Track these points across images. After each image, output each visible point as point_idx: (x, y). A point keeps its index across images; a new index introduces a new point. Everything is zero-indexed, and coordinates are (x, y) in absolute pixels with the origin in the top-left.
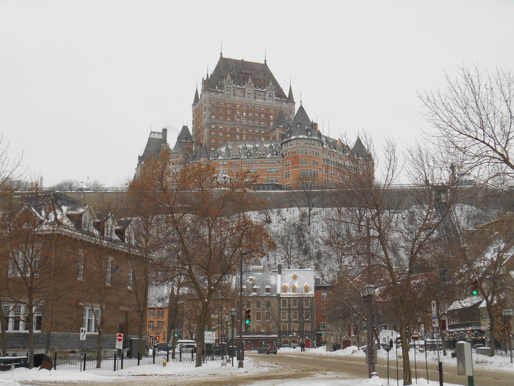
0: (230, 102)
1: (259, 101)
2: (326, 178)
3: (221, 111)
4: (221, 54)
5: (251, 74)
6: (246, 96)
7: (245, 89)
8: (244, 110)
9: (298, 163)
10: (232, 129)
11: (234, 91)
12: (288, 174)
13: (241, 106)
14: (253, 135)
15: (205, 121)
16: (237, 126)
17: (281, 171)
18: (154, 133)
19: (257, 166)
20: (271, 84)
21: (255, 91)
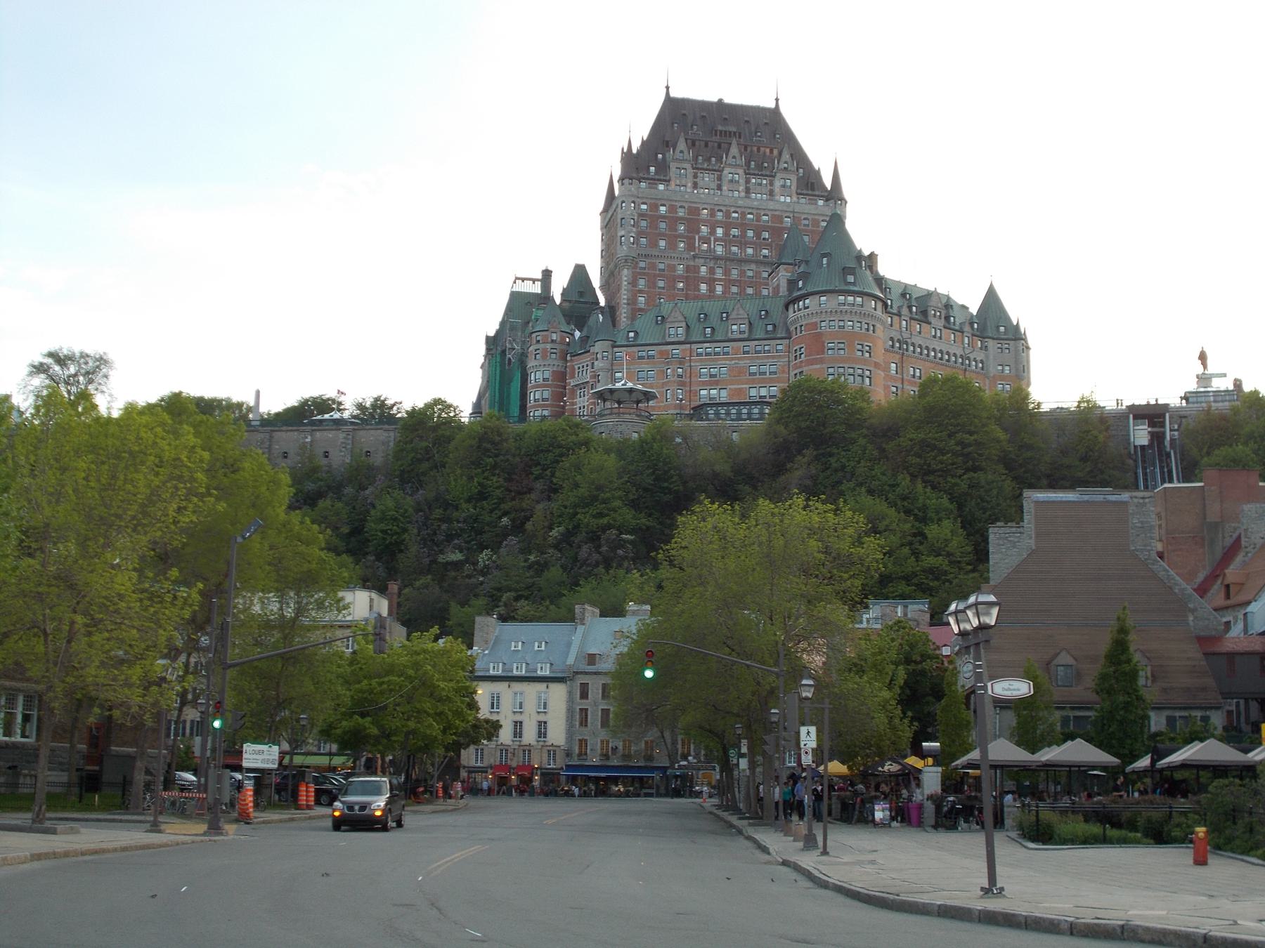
0: (684, 204)
1: (758, 197)
2: (900, 386)
3: (663, 225)
4: (667, 88)
5: (740, 134)
6: (725, 188)
8: (717, 222)
10: (688, 269)
11: (695, 176)
13: (712, 213)
14: (740, 281)
15: (622, 251)
16: (702, 261)
17: (783, 372)
18: (523, 280)
20: (786, 156)
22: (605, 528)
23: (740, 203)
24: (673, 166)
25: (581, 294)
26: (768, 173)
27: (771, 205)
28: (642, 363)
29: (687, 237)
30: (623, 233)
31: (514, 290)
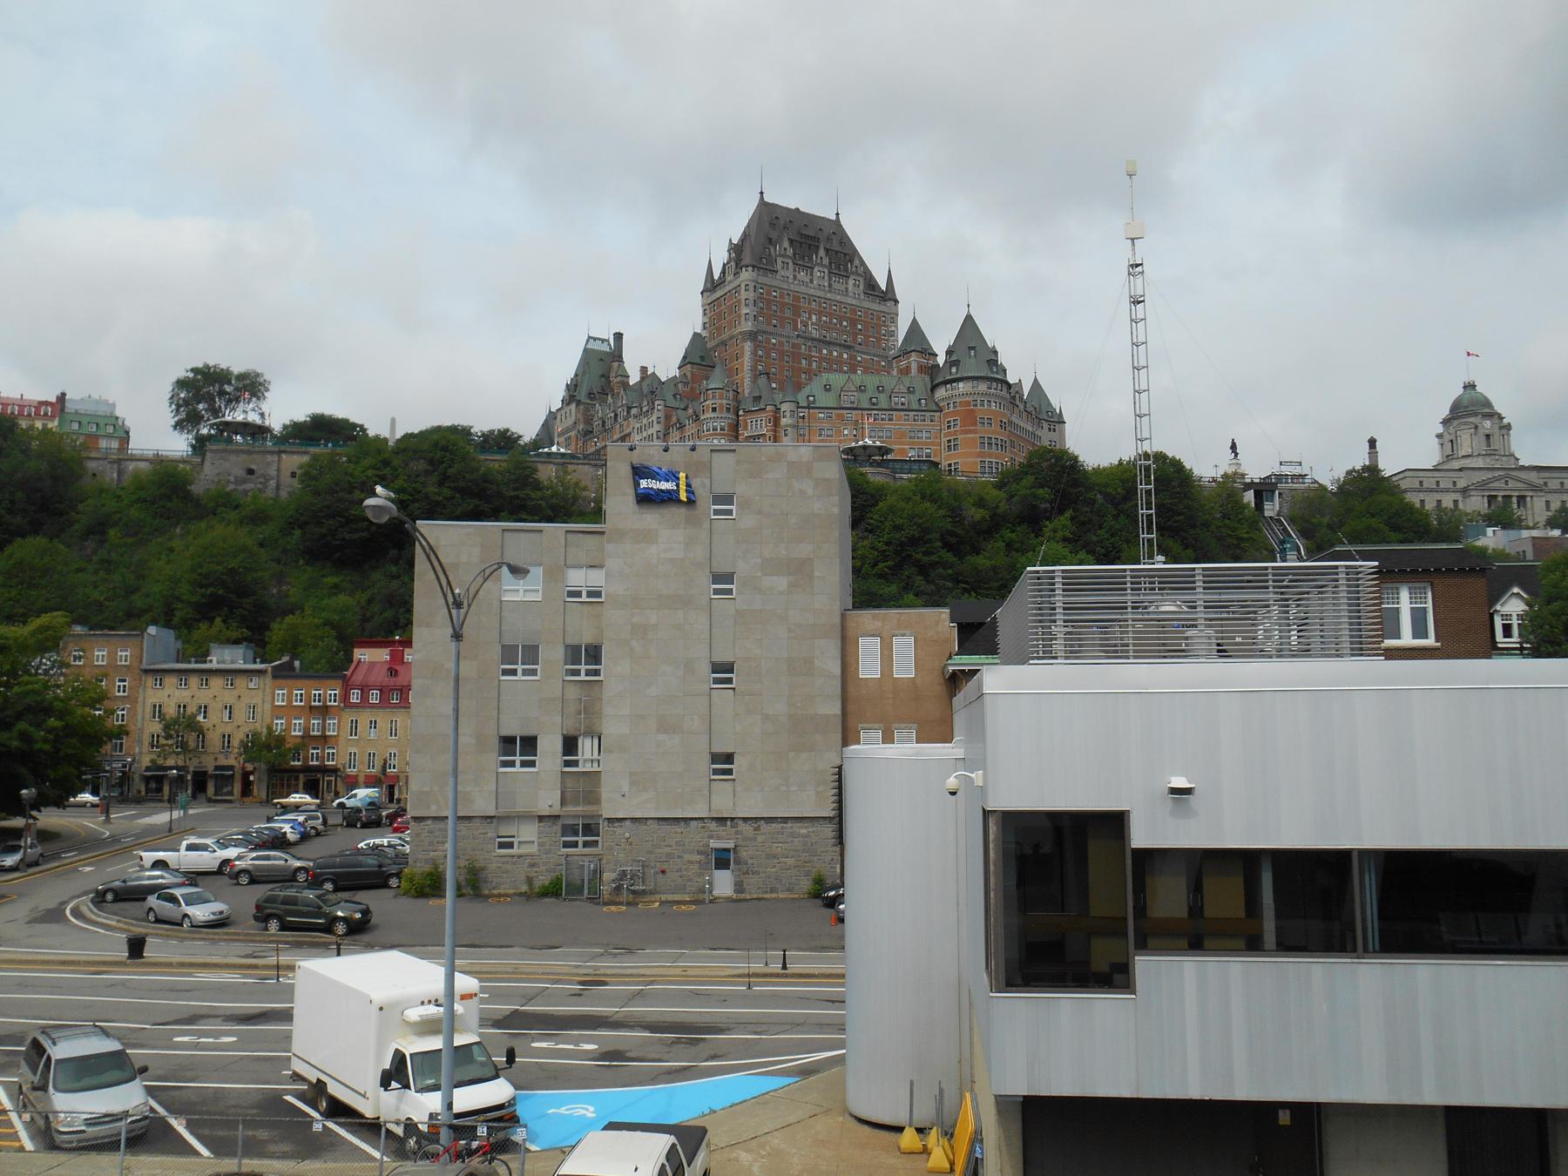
4: (762, 193)
6: (815, 282)
7: (813, 268)
9: (976, 425)
12: (952, 444)
15: (747, 326)
16: (803, 340)
18: (595, 339)
19: (892, 424)
20: (857, 262)
21: (830, 273)
22: (933, 565)
23: (829, 296)
24: (779, 260)
25: (702, 358)
26: (845, 274)
27: (850, 301)
28: (823, 423)
29: (792, 320)
30: (748, 311)
31: (588, 346)
